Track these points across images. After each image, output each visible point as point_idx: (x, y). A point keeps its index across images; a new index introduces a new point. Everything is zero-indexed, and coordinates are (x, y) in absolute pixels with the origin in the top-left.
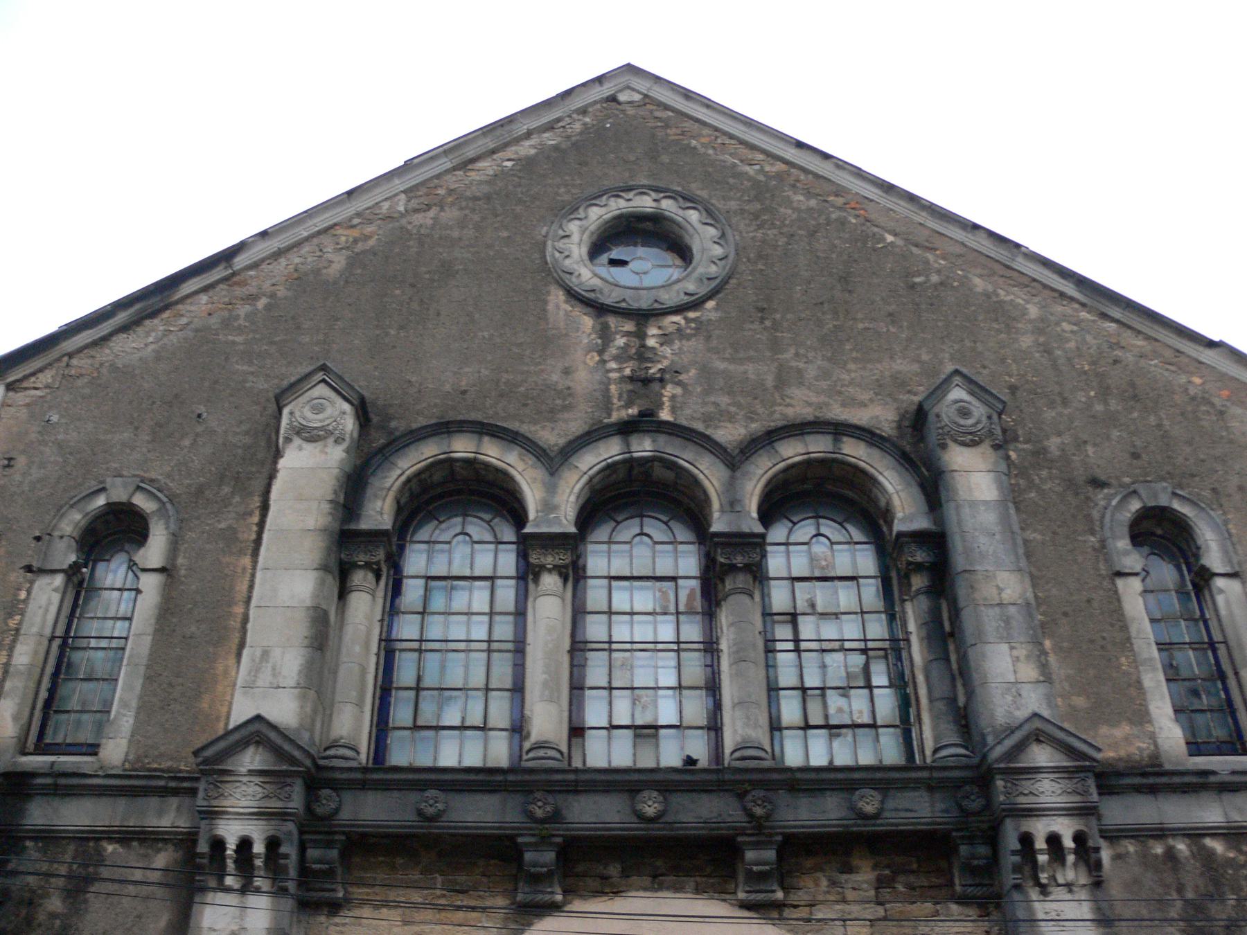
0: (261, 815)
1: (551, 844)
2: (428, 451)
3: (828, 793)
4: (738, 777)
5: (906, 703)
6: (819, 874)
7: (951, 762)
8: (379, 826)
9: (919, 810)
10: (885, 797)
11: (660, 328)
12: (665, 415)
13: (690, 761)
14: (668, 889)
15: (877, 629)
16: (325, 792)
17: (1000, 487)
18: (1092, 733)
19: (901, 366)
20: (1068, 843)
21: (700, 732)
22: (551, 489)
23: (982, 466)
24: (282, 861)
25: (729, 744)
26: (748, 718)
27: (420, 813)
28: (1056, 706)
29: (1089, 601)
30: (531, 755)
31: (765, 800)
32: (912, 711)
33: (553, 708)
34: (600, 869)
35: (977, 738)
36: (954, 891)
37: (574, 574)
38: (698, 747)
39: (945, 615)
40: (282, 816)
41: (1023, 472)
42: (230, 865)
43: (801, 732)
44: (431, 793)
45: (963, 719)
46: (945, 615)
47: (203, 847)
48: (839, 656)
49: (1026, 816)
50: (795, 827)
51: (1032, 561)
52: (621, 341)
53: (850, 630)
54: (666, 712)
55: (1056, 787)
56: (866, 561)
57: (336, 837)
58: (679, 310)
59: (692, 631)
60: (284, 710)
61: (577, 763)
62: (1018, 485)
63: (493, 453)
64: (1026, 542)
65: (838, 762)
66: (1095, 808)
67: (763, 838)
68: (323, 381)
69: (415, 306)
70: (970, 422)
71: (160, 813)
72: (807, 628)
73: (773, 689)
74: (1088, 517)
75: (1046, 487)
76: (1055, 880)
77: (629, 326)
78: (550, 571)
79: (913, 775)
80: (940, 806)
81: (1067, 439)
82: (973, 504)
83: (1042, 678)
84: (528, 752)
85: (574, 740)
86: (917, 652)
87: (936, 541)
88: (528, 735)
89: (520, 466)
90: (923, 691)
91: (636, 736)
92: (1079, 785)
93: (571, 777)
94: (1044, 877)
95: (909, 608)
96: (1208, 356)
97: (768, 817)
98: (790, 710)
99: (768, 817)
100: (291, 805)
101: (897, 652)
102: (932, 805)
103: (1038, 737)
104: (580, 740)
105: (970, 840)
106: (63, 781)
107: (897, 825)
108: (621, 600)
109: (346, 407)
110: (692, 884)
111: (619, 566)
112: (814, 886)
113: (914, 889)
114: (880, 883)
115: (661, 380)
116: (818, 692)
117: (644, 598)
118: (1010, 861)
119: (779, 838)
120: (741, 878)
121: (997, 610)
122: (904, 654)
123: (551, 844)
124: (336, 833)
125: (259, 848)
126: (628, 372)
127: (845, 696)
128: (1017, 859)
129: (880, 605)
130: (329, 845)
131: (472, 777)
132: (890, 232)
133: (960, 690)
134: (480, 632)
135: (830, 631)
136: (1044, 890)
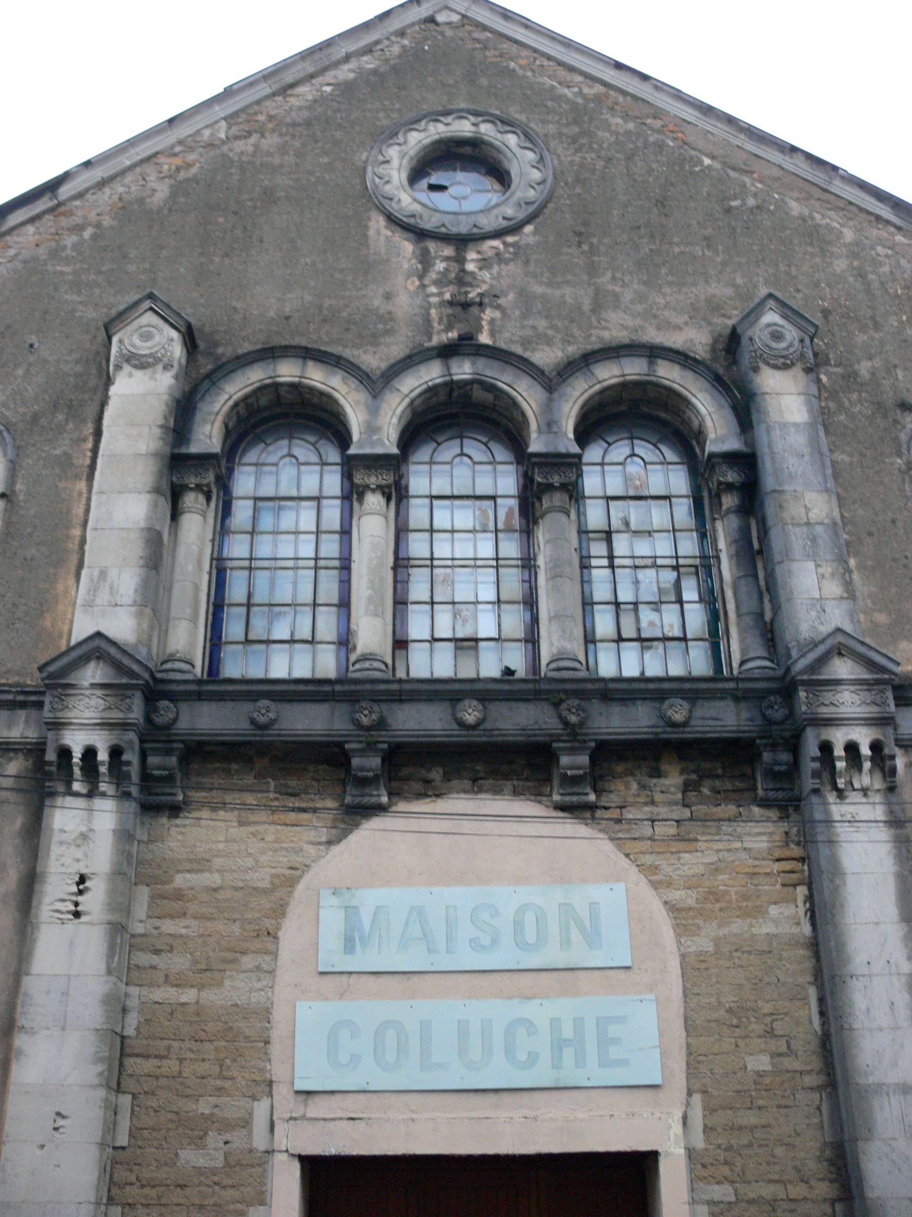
0: (104, 725)
1: (377, 750)
2: (254, 377)
3: (639, 702)
4: (554, 686)
5: (715, 618)
6: (630, 779)
7: (757, 674)
8: (217, 735)
9: (726, 719)
10: (693, 705)
11: (479, 252)
12: (484, 338)
13: (508, 672)
14: (487, 791)
15: (689, 546)
16: (164, 703)
17: (810, 410)
18: (891, 648)
19: (717, 290)
20: (865, 751)
21: (518, 644)
22: (374, 411)
23: (793, 389)
24: (125, 768)
25: (545, 655)
26: (564, 631)
27: (253, 721)
28: (859, 621)
29: (893, 522)
30: (357, 666)
31: (579, 708)
32: (721, 626)
33: (377, 622)
34: (423, 773)
35: (781, 649)
36: (756, 794)
37: (397, 494)
38: (517, 659)
39: (754, 534)
40: (124, 726)
41: (833, 395)
42: (77, 771)
43: (614, 645)
44: (264, 703)
45: (770, 634)
46: (754, 534)
47: (51, 756)
48: (651, 573)
49: (825, 725)
50: (608, 734)
51: (840, 483)
52: (440, 266)
53: (663, 547)
54: (486, 626)
55: (856, 698)
56: (678, 481)
57: (175, 745)
58: (498, 234)
59: (511, 548)
60: (122, 627)
61: (401, 674)
62: (827, 407)
63: (317, 377)
64: (833, 463)
65: (649, 673)
66: (892, 718)
67: (577, 745)
68: (151, 309)
69: (238, 233)
70: (783, 345)
71: (10, 726)
72: (621, 545)
73: (588, 603)
74: (896, 441)
75: (857, 409)
76: (852, 785)
77: (449, 251)
78: (373, 491)
79: (720, 685)
80: (745, 715)
81: (878, 362)
82: (784, 426)
83: (845, 595)
84: (353, 665)
85: (397, 652)
86: (727, 569)
87: (747, 462)
88: (355, 647)
89: (344, 389)
90: (731, 607)
91: (456, 648)
92: (878, 697)
93: (395, 687)
94: (841, 783)
95: (719, 526)
97: (582, 724)
98: (604, 624)
99: (582, 724)
100: (132, 715)
101: (708, 568)
102: (738, 714)
103: (840, 651)
104: (404, 652)
105: (774, 747)
107: (704, 733)
108: (442, 518)
109: (174, 334)
110: (510, 787)
111: (441, 485)
112: (624, 788)
113: (719, 792)
114: (687, 787)
115: (481, 304)
116: (631, 606)
117: (464, 516)
118: (809, 766)
119: (593, 744)
120: (556, 782)
121: (804, 529)
122: (714, 571)
123: (377, 750)
124: (175, 741)
125: (103, 756)
126: (447, 296)
127: (658, 610)
128: (816, 765)
129: (691, 523)
130: (168, 752)
131: (302, 687)
133: (767, 606)
134: (307, 549)
135: (643, 548)
136: (841, 794)
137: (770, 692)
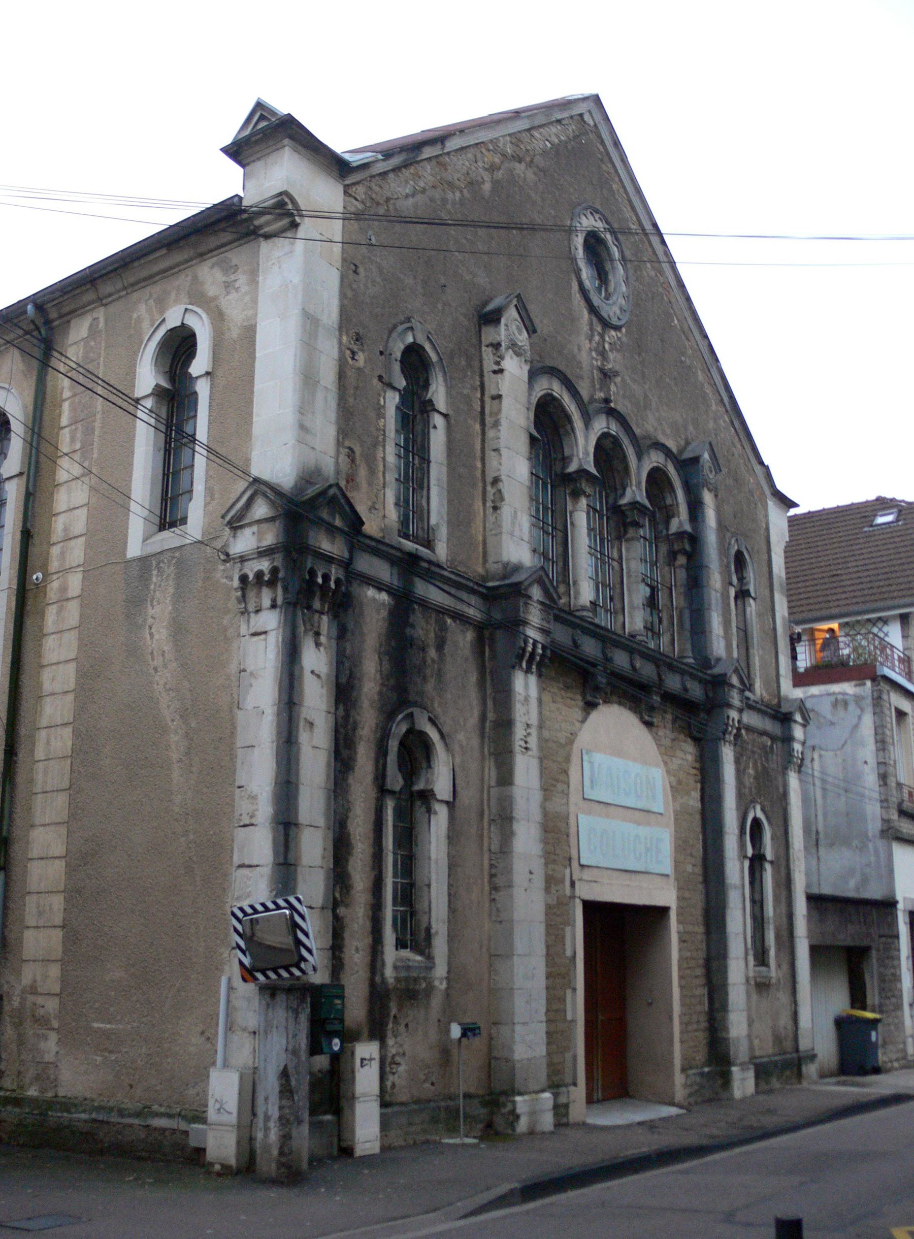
22: (586, 438)
96: (758, 469)
132: (678, 320)
137: (709, 682)
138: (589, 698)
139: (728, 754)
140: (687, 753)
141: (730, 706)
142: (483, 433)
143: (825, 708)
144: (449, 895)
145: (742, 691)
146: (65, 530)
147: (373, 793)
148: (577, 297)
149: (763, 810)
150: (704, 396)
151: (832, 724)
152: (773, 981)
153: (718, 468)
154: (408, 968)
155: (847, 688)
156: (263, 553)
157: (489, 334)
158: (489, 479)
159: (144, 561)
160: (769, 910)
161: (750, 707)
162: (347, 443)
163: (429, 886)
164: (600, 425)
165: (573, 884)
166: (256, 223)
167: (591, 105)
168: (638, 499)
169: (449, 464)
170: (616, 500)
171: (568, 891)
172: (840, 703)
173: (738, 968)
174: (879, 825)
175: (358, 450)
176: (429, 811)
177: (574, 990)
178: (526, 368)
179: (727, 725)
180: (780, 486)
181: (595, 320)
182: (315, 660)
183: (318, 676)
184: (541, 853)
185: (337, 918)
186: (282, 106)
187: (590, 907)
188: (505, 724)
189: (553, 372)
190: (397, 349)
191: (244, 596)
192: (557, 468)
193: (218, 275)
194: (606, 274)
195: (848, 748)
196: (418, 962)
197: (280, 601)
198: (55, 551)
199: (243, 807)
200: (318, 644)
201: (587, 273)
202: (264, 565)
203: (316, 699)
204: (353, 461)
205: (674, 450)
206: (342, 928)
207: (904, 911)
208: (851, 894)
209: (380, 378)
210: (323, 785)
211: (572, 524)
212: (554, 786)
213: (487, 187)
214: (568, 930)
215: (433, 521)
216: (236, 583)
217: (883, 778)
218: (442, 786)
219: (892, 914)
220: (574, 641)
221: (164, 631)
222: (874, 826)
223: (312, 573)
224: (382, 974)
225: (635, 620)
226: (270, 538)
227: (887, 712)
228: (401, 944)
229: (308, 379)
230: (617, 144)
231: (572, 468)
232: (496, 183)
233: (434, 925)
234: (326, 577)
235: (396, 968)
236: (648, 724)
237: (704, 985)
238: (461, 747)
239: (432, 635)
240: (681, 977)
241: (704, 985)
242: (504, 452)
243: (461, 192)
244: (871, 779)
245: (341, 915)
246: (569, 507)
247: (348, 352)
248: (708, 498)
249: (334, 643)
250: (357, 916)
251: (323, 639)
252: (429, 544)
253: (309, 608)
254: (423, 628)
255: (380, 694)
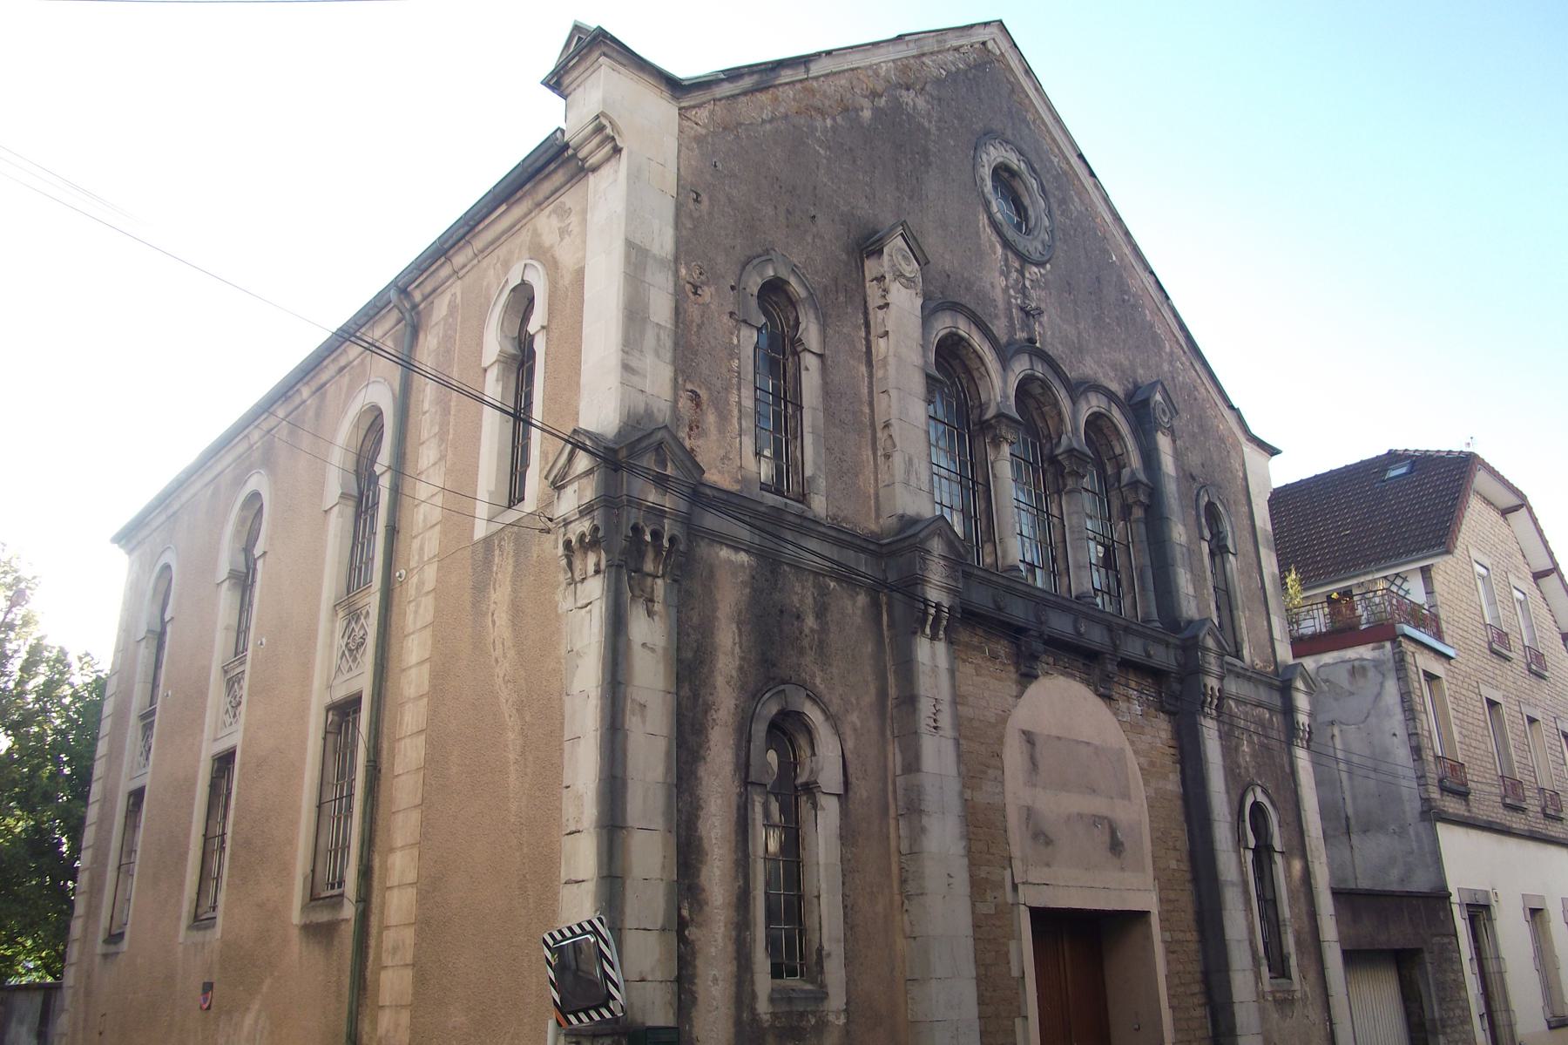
22: (1005, 382)
106: (805, 523)
138: (1023, 669)
139: (1210, 731)
140: (1160, 730)
141: (1207, 673)
142: (871, 376)
143: (1342, 678)
144: (845, 907)
145: (1220, 656)
146: (425, 518)
147: (734, 789)
148: (988, 232)
149: (1265, 791)
150: (1155, 337)
151: (1352, 694)
152: (1298, 995)
153: (1175, 412)
154: (790, 1000)
155: (1365, 652)
156: (585, 511)
157: (871, 267)
158: (879, 425)
159: (487, 541)
160: (1285, 911)
161: (1229, 671)
162: (689, 387)
163: (818, 897)
164: (1021, 366)
165: (1015, 887)
166: (581, 155)
167: (995, 29)
168: (1075, 445)
169: (825, 410)
170: (1052, 450)
171: (1010, 898)
172: (1357, 670)
173: (1244, 982)
174: (1418, 804)
175: (703, 393)
176: (815, 806)
177: (1026, 1018)
178: (919, 301)
179: (1205, 694)
180: (1255, 431)
181: (1010, 255)
182: (648, 631)
183: (653, 650)
184: (962, 852)
185: (682, 939)
186: (592, 23)
187: (1038, 915)
188: (909, 700)
189: (955, 307)
190: (754, 284)
191: (570, 565)
192: (974, 417)
193: (555, 222)
194: (1026, 210)
195: (1373, 720)
196: (811, 991)
197: (603, 566)
198: (416, 544)
199: (569, 811)
200: (650, 613)
201: (998, 206)
202: (585, 526)
203: (650, 675)
204: (698, 405)
205: (1121, 394)
206: (694, 954)
207: (1460, 905)
208: (1395, 887)
209: (731, 314)
210: (661, 779)
211: (995, 476)
212: (985, 773)
213: (867, 114)
214: (1013, 945)
215: (808, 473)
216: (561, 550)
217: (1417, 751)
218: (830, 778)
219: (1445, 909)
220: (995, 602)
221: (504, 615)
222: (1412, 808)
223: (636, 529)
224: (753, 1010)
225: (1087, 579)
226: (589, 495)
227: (1414, 677)
228: (776, 973)
229: (634, 315)
230: (1028, 71)
231: (990, 414)
232: (877, 111)
233: (826, 947)
234: (657, 535)
235: (772, 1000)
236: (1107, 698)
237: (1204, 1005)
238: (855, 730)
239: (810, 601)
240: (1171, 997)
241: (1204, 1005)
242: (893, 393)
243: (834, 119)
244: (1402, 754)
245: (692, 937)
246: (991, 457)
247: (688, 287)
248: (1164, 442)
249: (673, 611)
250: (714, 938)
251: (657, 607)
252: (803, 498)
253: (638, 570)
254: (801, 594)
255: (741, 668)
